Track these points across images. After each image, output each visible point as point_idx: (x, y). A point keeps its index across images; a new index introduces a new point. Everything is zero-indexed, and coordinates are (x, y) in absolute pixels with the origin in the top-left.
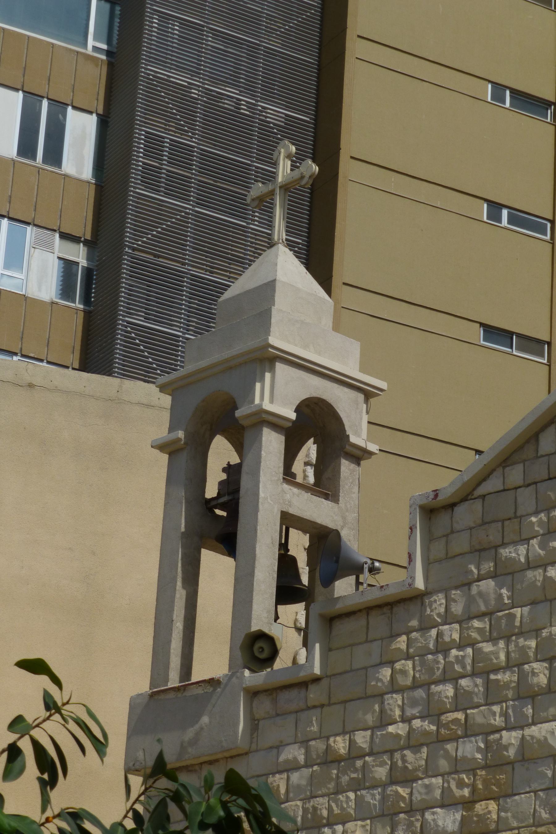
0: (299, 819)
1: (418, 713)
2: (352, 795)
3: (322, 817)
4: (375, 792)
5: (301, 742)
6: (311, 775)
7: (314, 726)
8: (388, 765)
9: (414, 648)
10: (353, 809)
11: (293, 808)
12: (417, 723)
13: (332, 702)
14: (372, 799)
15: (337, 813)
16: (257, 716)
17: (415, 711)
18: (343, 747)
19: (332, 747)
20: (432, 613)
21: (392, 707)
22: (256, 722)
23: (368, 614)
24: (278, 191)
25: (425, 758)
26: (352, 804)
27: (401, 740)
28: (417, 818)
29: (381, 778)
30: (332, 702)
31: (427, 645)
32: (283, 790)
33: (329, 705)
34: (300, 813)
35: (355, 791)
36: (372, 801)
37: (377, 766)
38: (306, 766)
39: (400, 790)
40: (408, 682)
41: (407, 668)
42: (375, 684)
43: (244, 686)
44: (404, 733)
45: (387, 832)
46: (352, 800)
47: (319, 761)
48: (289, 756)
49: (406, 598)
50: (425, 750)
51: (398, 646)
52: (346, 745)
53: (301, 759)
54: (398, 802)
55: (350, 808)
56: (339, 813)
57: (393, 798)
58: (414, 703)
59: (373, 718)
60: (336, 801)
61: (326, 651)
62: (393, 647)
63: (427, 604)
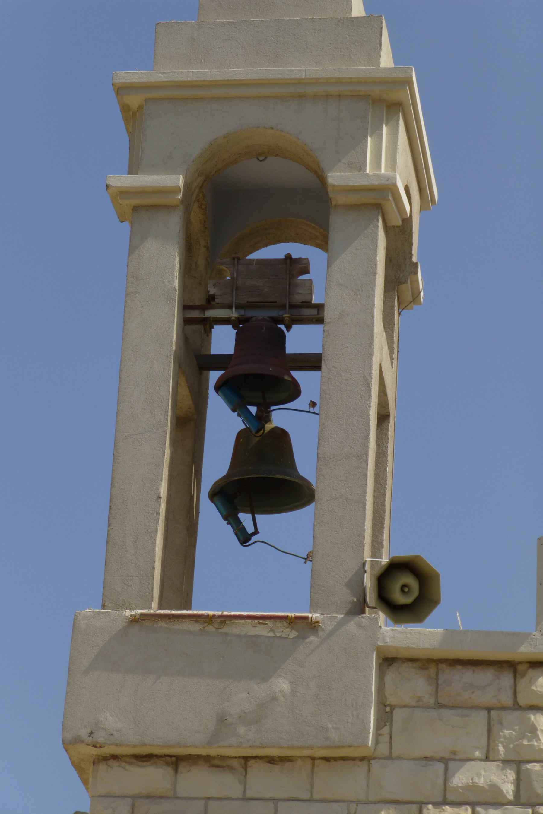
5: (506, 762)
16: (391, 700)
22: (388, 709)
43: (380, 643)
48: (476, 780)
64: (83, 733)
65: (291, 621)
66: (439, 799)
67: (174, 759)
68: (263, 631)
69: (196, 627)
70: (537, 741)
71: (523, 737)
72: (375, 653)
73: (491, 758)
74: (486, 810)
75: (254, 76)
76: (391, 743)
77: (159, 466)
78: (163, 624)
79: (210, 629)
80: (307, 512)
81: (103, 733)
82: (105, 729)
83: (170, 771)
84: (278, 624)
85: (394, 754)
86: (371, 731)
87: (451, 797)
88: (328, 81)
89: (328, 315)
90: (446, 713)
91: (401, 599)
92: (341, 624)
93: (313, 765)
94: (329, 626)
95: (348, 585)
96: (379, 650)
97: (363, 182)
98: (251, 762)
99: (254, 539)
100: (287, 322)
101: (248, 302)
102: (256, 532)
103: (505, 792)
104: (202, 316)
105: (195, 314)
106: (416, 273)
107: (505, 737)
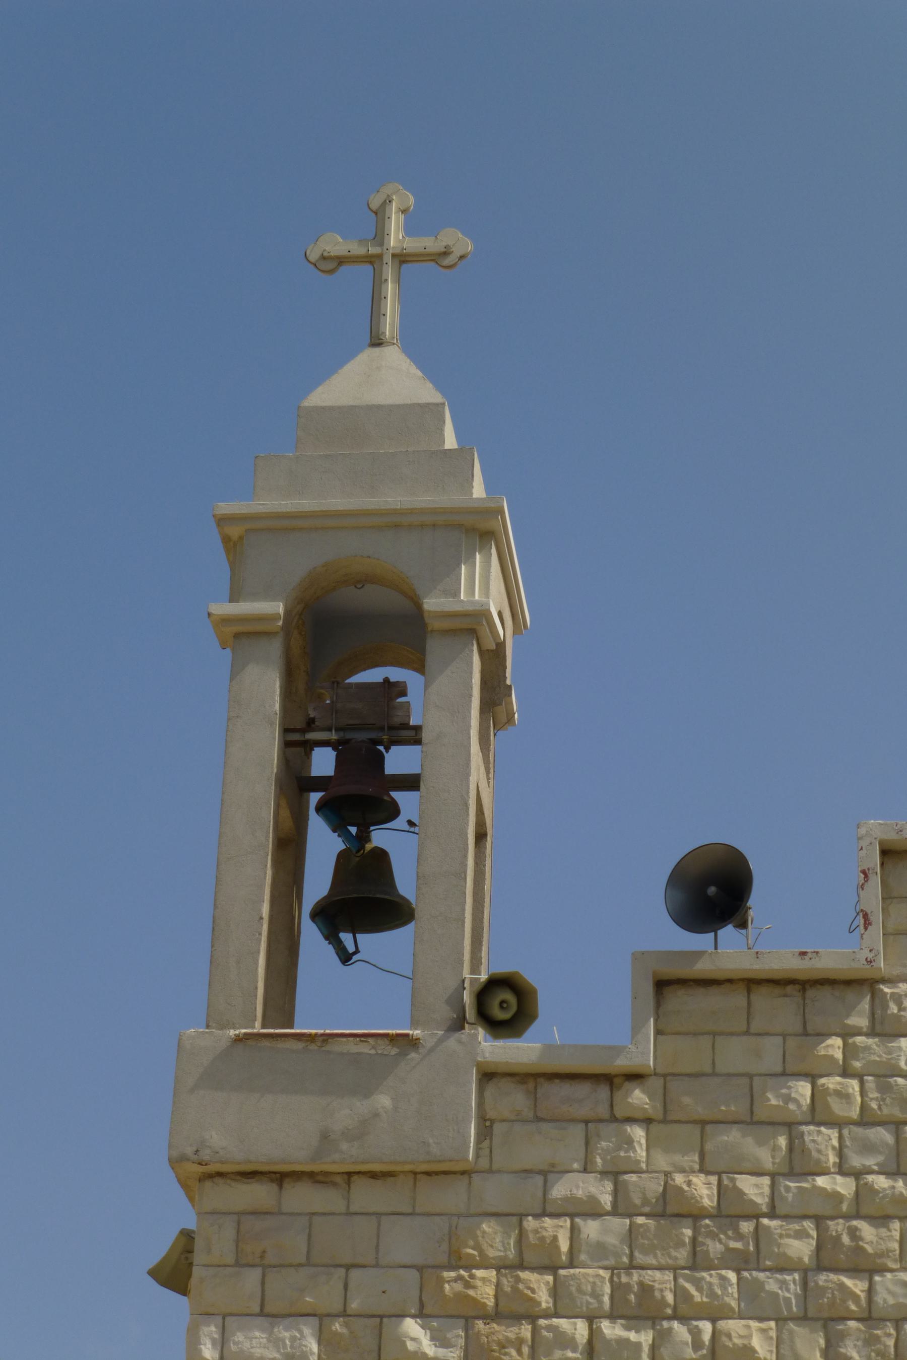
0: (606, 1299)
1: (874, 1165)
2: (732, 1276)
3: (663, 1303)
4: (788, 1278)
5: (604, 1174)
6: (630, 1230)
7: (636, 1151)
8: (813, 1238)
9: (864, 1062)
10: (734, 1299)
11: (591, 1280)
12: (881, 1182)
13: (670, 1117)
14: (781, 1288)
15: (699, 1300)
16: (491, 1114)
17: (871, 1162)
18: (708, 1195)
19: (686, 1192)
20: (902, 1013)
21: (822, 1147)
22: (488, 1123)
23: (749, 991)
24: (388, 258)
25: (898, 1238)
26: (733, 1290)
27: (841, 1202)
28: (888, 1331)
29: (800, 1259)
30: (670, 1117)
31: (893, 1062)
32: (564, 1246)
33: (664, 1121)
34: (607, 1289)
35: (738, 1271)
36: (780, 1292)
37: (789, 1236)
38: (615, 1212)
39: (848, 1282)
40: (853, 1113)
41: (851, 1091)
42: (781, 1103)
43: (479, 1059)
44: (849, 1194)
45: (819, 1346)
46: (732, 1284)
47: (647, 1209)
49: (834, 980)
50: (896, 1225)
51: (830, 1052)
52: (712, 1193)
53: (606, 1200)
54: (844, 1301)
55: (729, 1296)
56: (706, 1303)
57: (833, 1294)
58: (868, 1148)
59: (773, 1157)
60: (697, 1284)
61: (658, 1032)
62: (823, 1053)
63: (888, 998)
64: (189, 1151)
65: (393, 1039)
66: (539, 1211)
67: (278, 1175)
68: (364, 1048)
69: (299, 1045)
70: (633, 1153)
71: (619, 1148)
72: (475, 1068)
73: (588, 1170)
74: (585, 1220)
75: (351, 507)
76: (491, 1156)
77: (261, 887)
78: (266, 1043)
79: (313, 1047)
80: (408, 930)
81: (208, 1151)
82: (210, 1147)
83: (274, 1187)
84: (380, 1041)
85: (495, 1167)
86: (472, 1145)
87: (549, 1209)
88: (422, 511)
89: (426, 736)
90: (544, 1126)
91: (500, 1015)
92: (441, 1041)
93: (415, 1179)
94: (429, 1043)
95: (448, 1002)
96: (479, 1065)
97: (457, 608)
98: (355, 1178)
99: (355, 958)
100: (386, 744)
101: (347, 725)
102: (357, 951)
103: (603, 1203)
104: (302, 739)
105: (296, 737)
106: (510, 695)
107: (602, 1149)
